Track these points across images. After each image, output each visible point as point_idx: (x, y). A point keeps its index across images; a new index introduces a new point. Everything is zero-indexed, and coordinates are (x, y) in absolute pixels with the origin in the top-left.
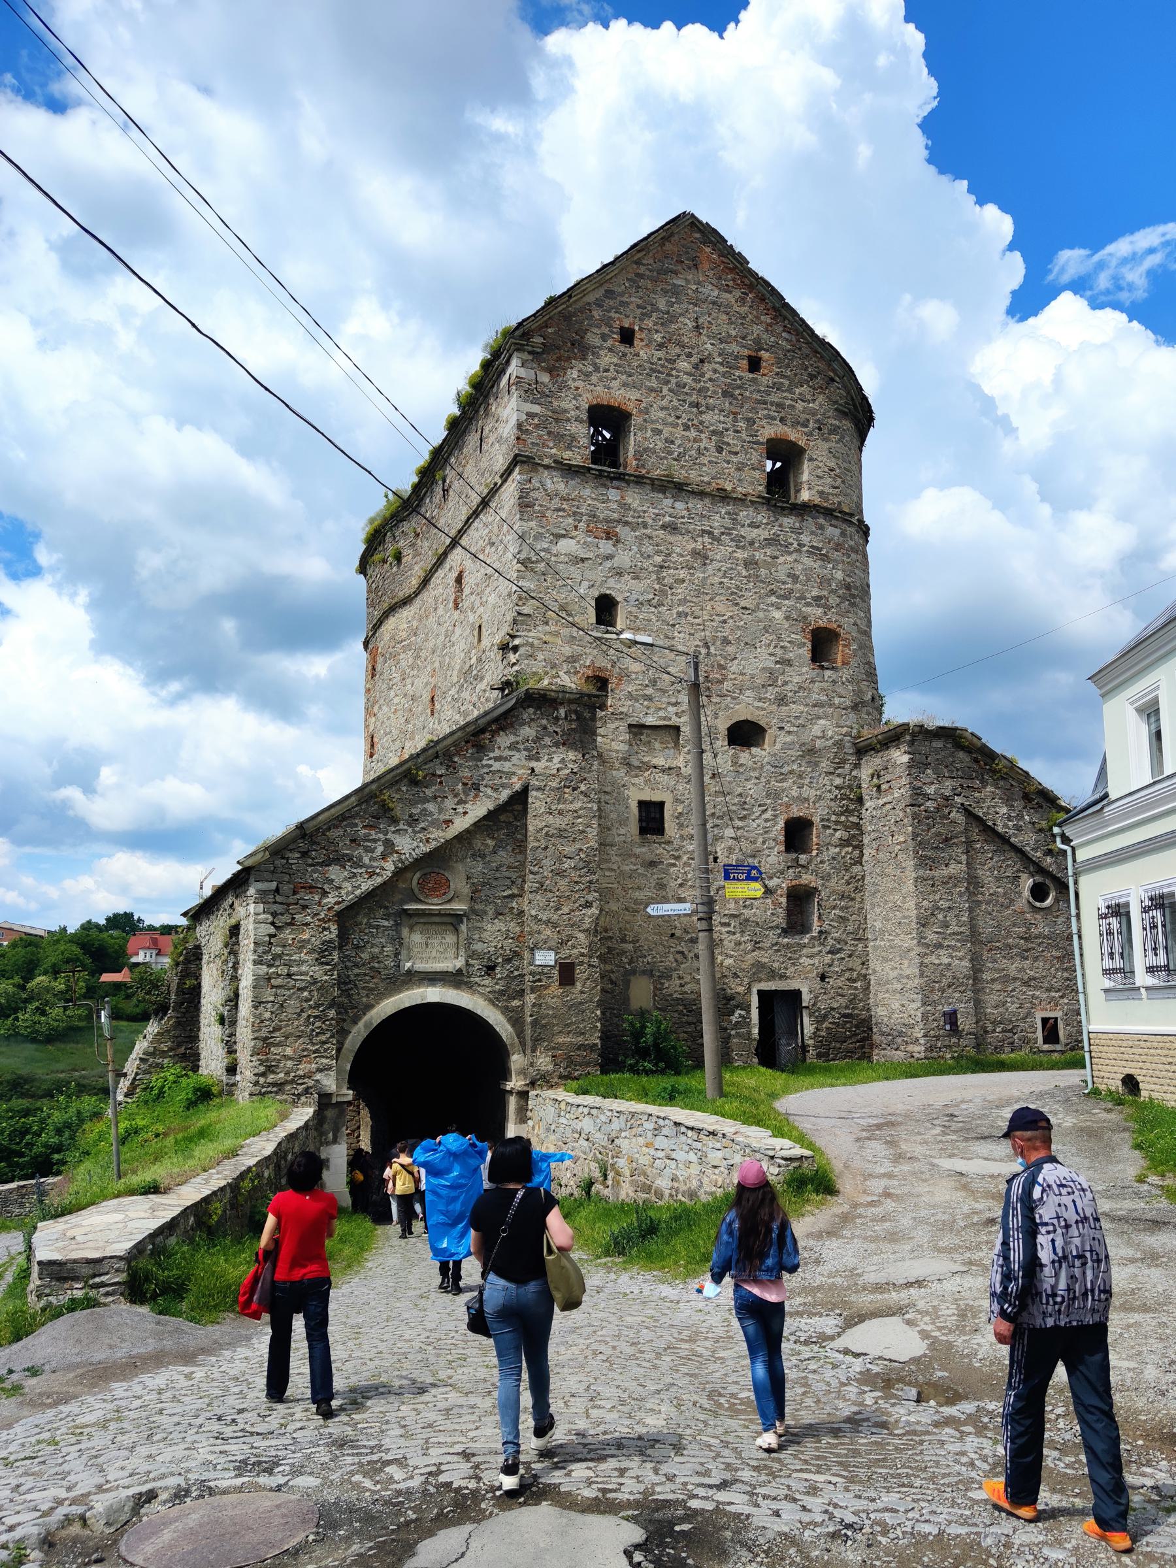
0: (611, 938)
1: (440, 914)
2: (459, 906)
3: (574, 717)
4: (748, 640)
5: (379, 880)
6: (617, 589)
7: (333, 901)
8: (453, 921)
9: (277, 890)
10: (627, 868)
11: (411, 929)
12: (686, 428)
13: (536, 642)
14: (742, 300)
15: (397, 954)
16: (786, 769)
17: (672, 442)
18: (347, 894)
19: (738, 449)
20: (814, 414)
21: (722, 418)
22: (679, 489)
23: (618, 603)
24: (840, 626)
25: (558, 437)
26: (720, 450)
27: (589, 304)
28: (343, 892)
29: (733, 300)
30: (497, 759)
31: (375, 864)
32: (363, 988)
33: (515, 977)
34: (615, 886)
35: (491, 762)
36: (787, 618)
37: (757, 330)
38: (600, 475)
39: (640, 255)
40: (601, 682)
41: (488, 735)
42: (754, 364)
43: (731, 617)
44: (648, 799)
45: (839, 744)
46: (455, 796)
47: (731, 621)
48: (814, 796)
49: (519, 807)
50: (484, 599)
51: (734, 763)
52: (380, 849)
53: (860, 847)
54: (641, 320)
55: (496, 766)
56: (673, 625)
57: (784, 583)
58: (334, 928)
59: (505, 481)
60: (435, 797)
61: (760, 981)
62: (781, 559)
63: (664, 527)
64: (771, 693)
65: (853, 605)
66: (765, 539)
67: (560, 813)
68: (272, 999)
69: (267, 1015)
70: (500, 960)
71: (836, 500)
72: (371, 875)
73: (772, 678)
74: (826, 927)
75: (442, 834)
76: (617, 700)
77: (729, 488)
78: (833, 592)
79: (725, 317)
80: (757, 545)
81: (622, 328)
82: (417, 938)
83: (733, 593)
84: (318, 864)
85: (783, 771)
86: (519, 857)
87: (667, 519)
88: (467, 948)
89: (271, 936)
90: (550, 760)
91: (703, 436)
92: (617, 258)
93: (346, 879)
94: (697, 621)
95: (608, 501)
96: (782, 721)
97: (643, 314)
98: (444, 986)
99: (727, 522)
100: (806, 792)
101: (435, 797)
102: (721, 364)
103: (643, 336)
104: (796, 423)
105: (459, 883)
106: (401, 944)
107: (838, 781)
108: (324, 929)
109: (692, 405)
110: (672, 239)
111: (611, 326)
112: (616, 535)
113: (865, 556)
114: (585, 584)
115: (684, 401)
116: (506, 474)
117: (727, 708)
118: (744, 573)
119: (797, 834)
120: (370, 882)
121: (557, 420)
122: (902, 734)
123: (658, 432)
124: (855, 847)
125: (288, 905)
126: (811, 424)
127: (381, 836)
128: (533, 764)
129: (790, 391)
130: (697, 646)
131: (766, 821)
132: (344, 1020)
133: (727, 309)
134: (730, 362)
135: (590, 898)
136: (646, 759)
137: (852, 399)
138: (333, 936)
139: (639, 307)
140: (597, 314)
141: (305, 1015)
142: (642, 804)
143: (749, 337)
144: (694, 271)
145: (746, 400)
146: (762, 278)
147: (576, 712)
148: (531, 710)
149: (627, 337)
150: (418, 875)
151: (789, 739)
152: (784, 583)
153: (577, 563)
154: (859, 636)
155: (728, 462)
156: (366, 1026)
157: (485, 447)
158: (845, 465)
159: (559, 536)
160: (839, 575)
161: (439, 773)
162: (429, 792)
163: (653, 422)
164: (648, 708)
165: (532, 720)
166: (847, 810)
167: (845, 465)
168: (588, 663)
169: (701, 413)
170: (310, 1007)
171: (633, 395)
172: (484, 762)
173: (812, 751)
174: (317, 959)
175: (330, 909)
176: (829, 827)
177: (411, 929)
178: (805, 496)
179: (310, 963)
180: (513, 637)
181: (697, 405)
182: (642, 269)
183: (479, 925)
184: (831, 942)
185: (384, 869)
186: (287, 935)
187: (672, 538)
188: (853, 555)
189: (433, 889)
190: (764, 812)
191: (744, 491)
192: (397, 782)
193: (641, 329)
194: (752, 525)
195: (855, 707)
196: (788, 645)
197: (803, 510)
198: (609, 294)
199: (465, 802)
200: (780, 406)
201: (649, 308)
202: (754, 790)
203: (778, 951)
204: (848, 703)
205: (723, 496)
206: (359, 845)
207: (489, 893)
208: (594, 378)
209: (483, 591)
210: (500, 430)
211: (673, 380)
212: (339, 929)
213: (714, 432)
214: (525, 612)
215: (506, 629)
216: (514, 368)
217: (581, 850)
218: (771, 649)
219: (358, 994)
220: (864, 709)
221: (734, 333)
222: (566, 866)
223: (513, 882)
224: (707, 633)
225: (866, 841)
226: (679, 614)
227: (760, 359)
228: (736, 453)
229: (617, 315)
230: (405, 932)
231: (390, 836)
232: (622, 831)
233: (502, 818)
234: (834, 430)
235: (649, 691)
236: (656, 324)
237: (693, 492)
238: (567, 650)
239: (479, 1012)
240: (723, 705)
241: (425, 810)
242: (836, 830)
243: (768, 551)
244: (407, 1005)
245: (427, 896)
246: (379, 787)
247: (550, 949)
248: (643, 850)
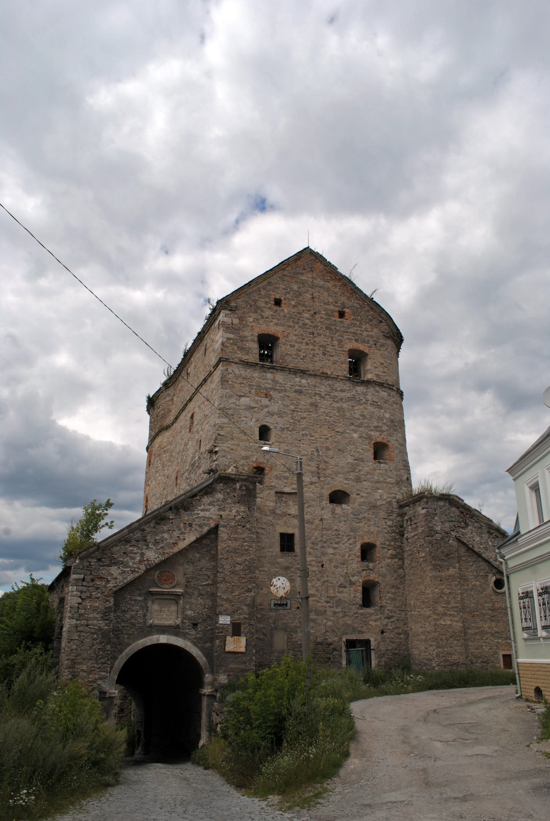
0: (263, 609)
1: (169, 594)
2: (179, 590)
3: (244, 488)
4: (340, 448)
5: (137, 575)
7: (112, 585)
8: (175, 598)
9: (84, 580)
10: (273, 570)
11: (153, 602)
12: (307, 344)
13: (227, 449)
14: (335, 286)
15: (145, 616)
16: (361, 516)
17: (300, 351)
18: (120, 582)
19: (334, 354)
20: (372, 338)
21: (325, 340)
22: (303, 373)
23: (271, 429)
24: (389, 441)
25: (241, 349)
26: (324, 354)
27: (259, 288)
28: (118, 581)
29: (331, 286)
30: (202, 510)
31: (135, 566)
32: (126, 634)
33: (208, 630)
34: (266, 580)
35: (199, 512)
36: (360, 437)
37: (343, 299)
38: (263, 366)
39: (284, 266)
40: (260, 470)
41: (198, 498)
42: (342, 315)
43: (331, 436)
44: (285, 532)
45: (390, 503)
46: (179, 530)
47: (330, 438)
48: (376, 531)
49: (213, 536)
50: (203, 427)
51: (333, 513)
52: (138, 558)
53: (402, 559)
54: (285, 295)
55: (202, 514)
56: (300, 441)
57: (359, 419)
58: (112, 600)
59: (215, 370)
60: (169, 530)
61: (347, 634)
62: (356, 408)
63: (296, 391)
64: (352, 476)
65: (395, 430)
66: (348, 398)
67: (236, 539)
68: (77, 638)
69: (74, 647)
70: (200, 620)
71: (385, 378)
72: (133, 572)
73: (353, 468)
74: (384, 604)
75: (171, 551)
76: (270, 479)
77: (329, 373)
78: (384, 423)
79: (326, 293)
80: (344, 400)
81: (275, 299)
82: (156, 607)
83: (332, 424)
84: (105, 565)
85: (359, 517)
86: (213, 564)
87: (298, 388)
88: (183, 612)
89: (79, 604)
90: (231, 511)
91: (316, 348)
92: (273, 268)
93: (119, 574)
94: (312, 438)
95: (266, 379)
96: (358, 490)
97: (286, 292)
98: (169, 634)
99: (328, 389)
100: (373, 529)
101: (169, 530)
102: (325, 314)
103: (286, 302)
104: (363, 342)
105: (180, 578)
106: (147, 610)
107: (390, 523)
108: (107, 601)
109: (310, 333)
110: (301, 260)
111: (270, 298)
112: (271, 395)
113: (401, 408)
114: (254, 420)
115: (306, 331)
116: (216, 366)
117: (328, 484)
118: (337, 414)
119: (367, 552)
120: (132, 576)
121: (242, 341)
122: (422, 498)
123: (292, 346)
124: (399, 559)
125: (89, 587)
126: (371, 342)
127: (139, 551)
128: (222, 513)
129: (360, 327)
130: (313, 451)
131: (350, 544)
132: (115, 651)
133: (328, 290)
134: (329, 315)
135: (250, 587)
136: (285, 510)
137: (392, 331)
138: (111, 605)
139: (284, 289)
140: (263, 292)
141: (94, 647)
142: (282, 535)
143: (339, 302)
144: (311, 273)
145: (337, 331)
146: (344, 276)
147: (245, 486)
148: (221, 485)
149: (278, 302)
150: (158, 572)
151: (362, 500)
153: (250, 409)
154: (399, 446)
155: (329, 360)
156: (126, 655)
157: (207, 354)
158: (389, 361)
159: (241, 396)
160: (387, 415)
161: (171, 517)
162: (165, 528)
163: (290, 342)
164: (286, 483)
165: (222, 490)
166: (395, 539)
167: (389, 361)
168: (254, 460)
169: (315, 337)
170: (97, 643)
171: (280, 329)
172: (196, 512)
173: (374, 507)
174: (102, 617)
175: (110, 590)
176: (385, 548)
177: (153, 602)
178: (369, 376)
179: (99, 619)
180: (215, 446)
181: (313, 333)
182: (286, 273)
183: (189, 600)
184: (387, 612)
185: (140, 569)
186: (88, 603)
187: (299, 397)
188: (395, 406)
189: (165, 580)
190: (349, 539)
191: (337, 374)
192: (149, 522)
193: (285, 299)
194: (342, 391)
195: (397, 483)
196: (361, 451)
197: (368, 383)
198: (269, 284)
199: (185, 533)
200: (355, 334)
201: (289, 290)
202: (343, 527)
203: (357, 617)
204: (394, 481)
205: (325, 376)
206: (127, 556)
207: (196, 583)
208: (261, 321)
209: (202, 424)
210: (214, 346)
212: (115, 601)
213: (321, 346)
214: (222, 434)
215: (212, 443)
216: (222, 317)
217: (246, 560)
218: (352, 453)
219: (123, 637)
220: (403, 484)
221: (331, 300)
222: (238, 568)
223: (209, 577)
224: (318, 445)
225: (405, 556)
226: (303, 435)
227: (345, 312)
228: (333, 356)
229: (273, 293)
230: (150, 604)
231: (144, 551)
232: (271, 550)
233: (204, 542)
234: (383, 345)
235: (287, 474)
236: (293, 296)
237: (311, 375)
238: (243, 453)
239: (188, 649)
240: (326, 482)
241: (163, 537)
242: (389, 550)
243: (350, 404)
244: (149, 644)
245: (162, 584)
246: (139, 525)
247: (228, 615)
248: (282, 560)
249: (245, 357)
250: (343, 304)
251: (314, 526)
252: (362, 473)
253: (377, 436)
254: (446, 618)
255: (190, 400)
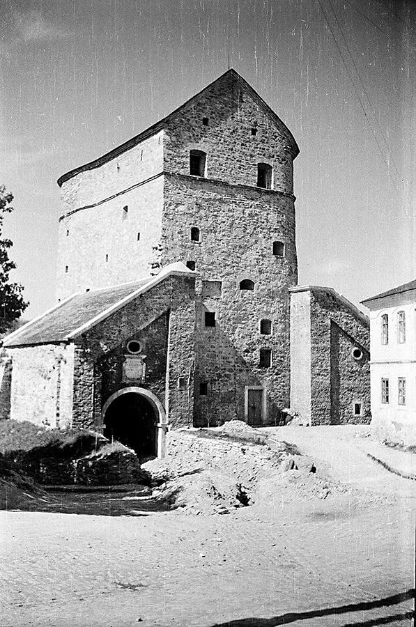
6: (201, 225)
42: (254, 132)
126: (275, 157)
152: (263, 223)
159: (178, 204)
164: (210, 274)
211: (222, 139)
235: (211, 267)
249: (182, 172)
250: (256, 123)
251: (229, 306)
252: (264, 266)
253: (276, 237)
254: (320, 377)
255: (123, 193)
